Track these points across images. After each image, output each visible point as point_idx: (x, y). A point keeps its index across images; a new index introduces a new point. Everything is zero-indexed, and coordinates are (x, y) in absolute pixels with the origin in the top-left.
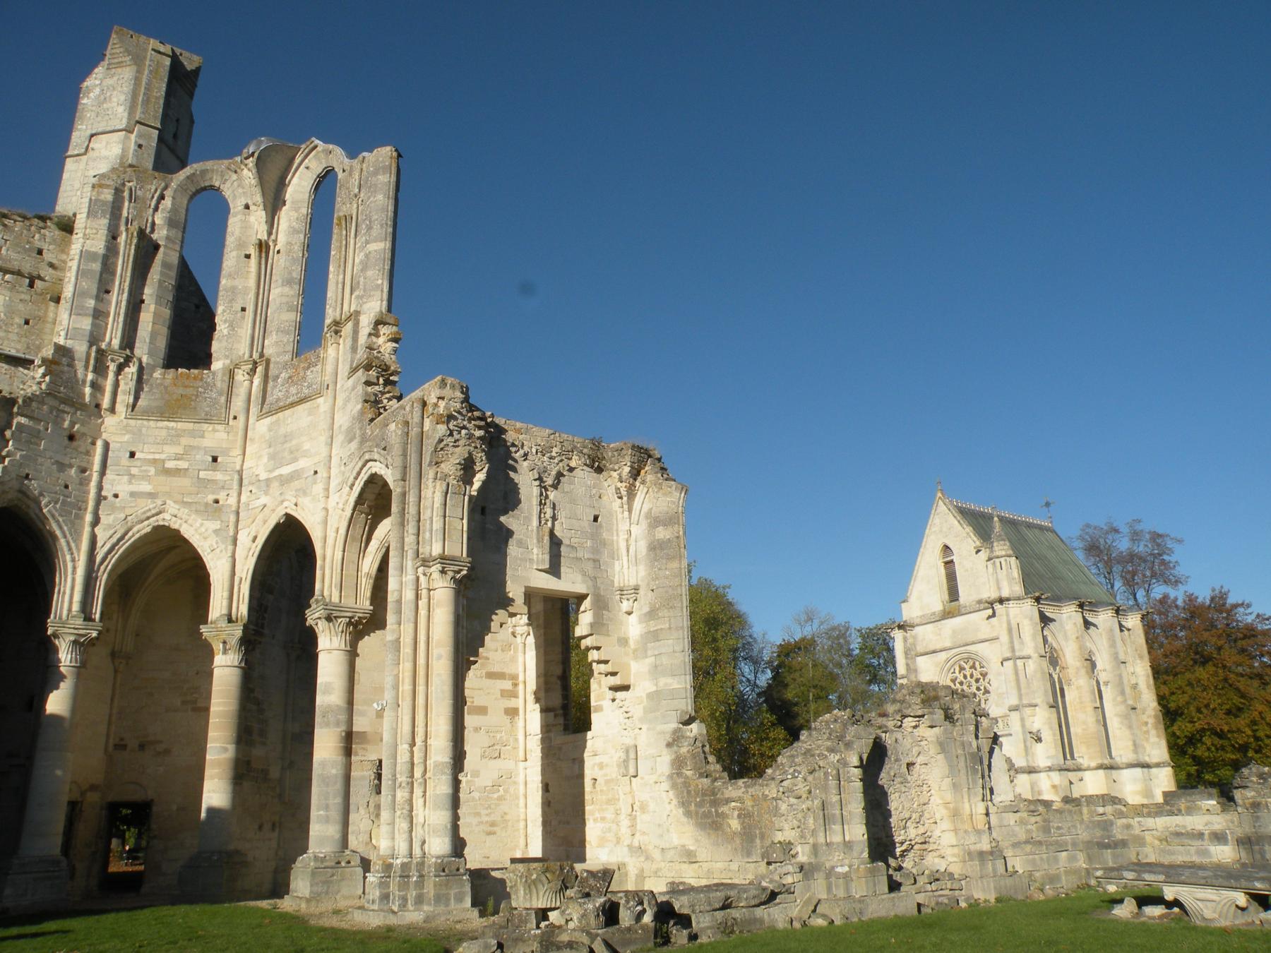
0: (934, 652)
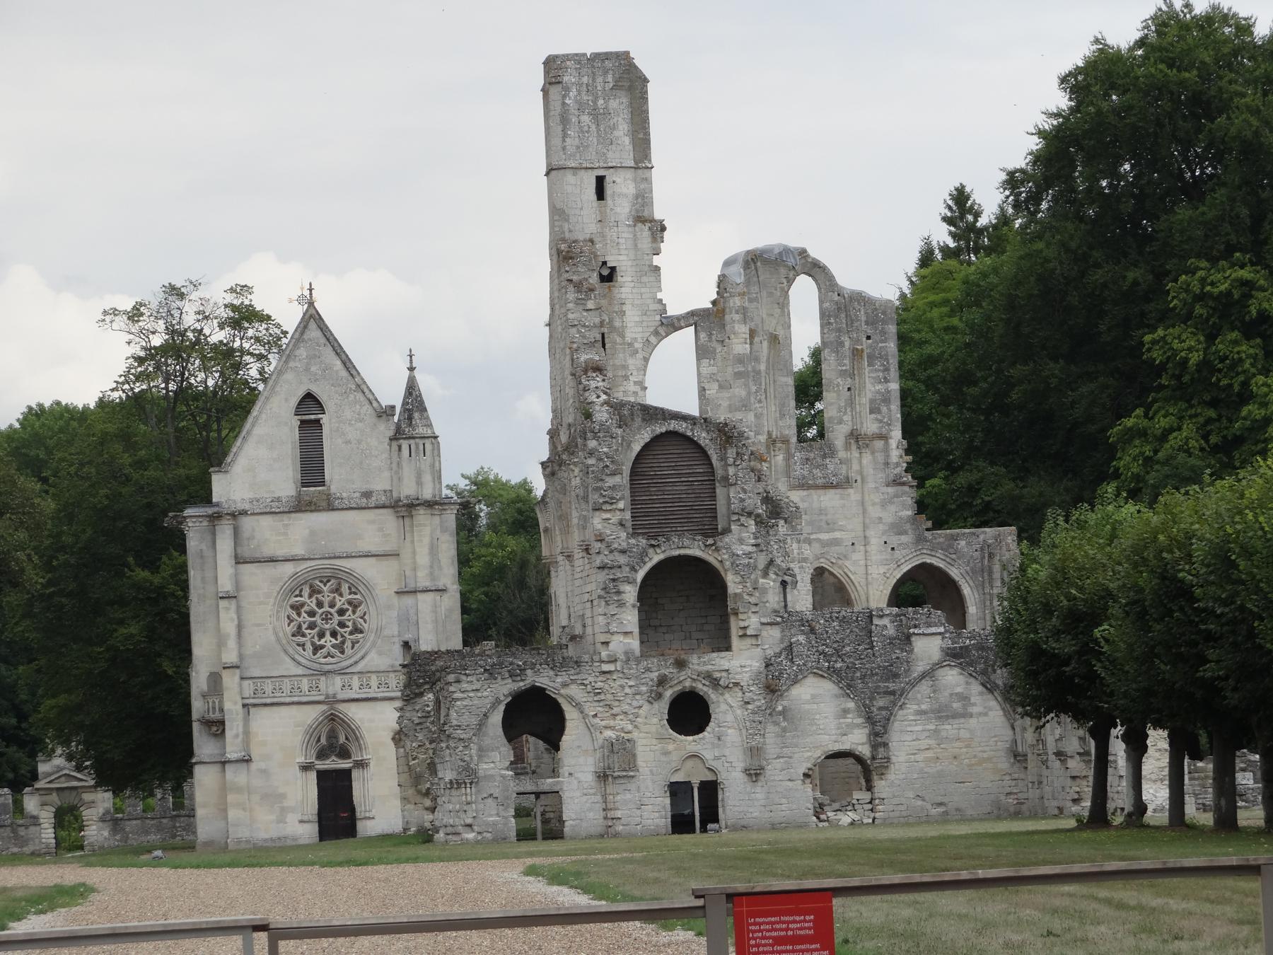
0: (273, 560)
